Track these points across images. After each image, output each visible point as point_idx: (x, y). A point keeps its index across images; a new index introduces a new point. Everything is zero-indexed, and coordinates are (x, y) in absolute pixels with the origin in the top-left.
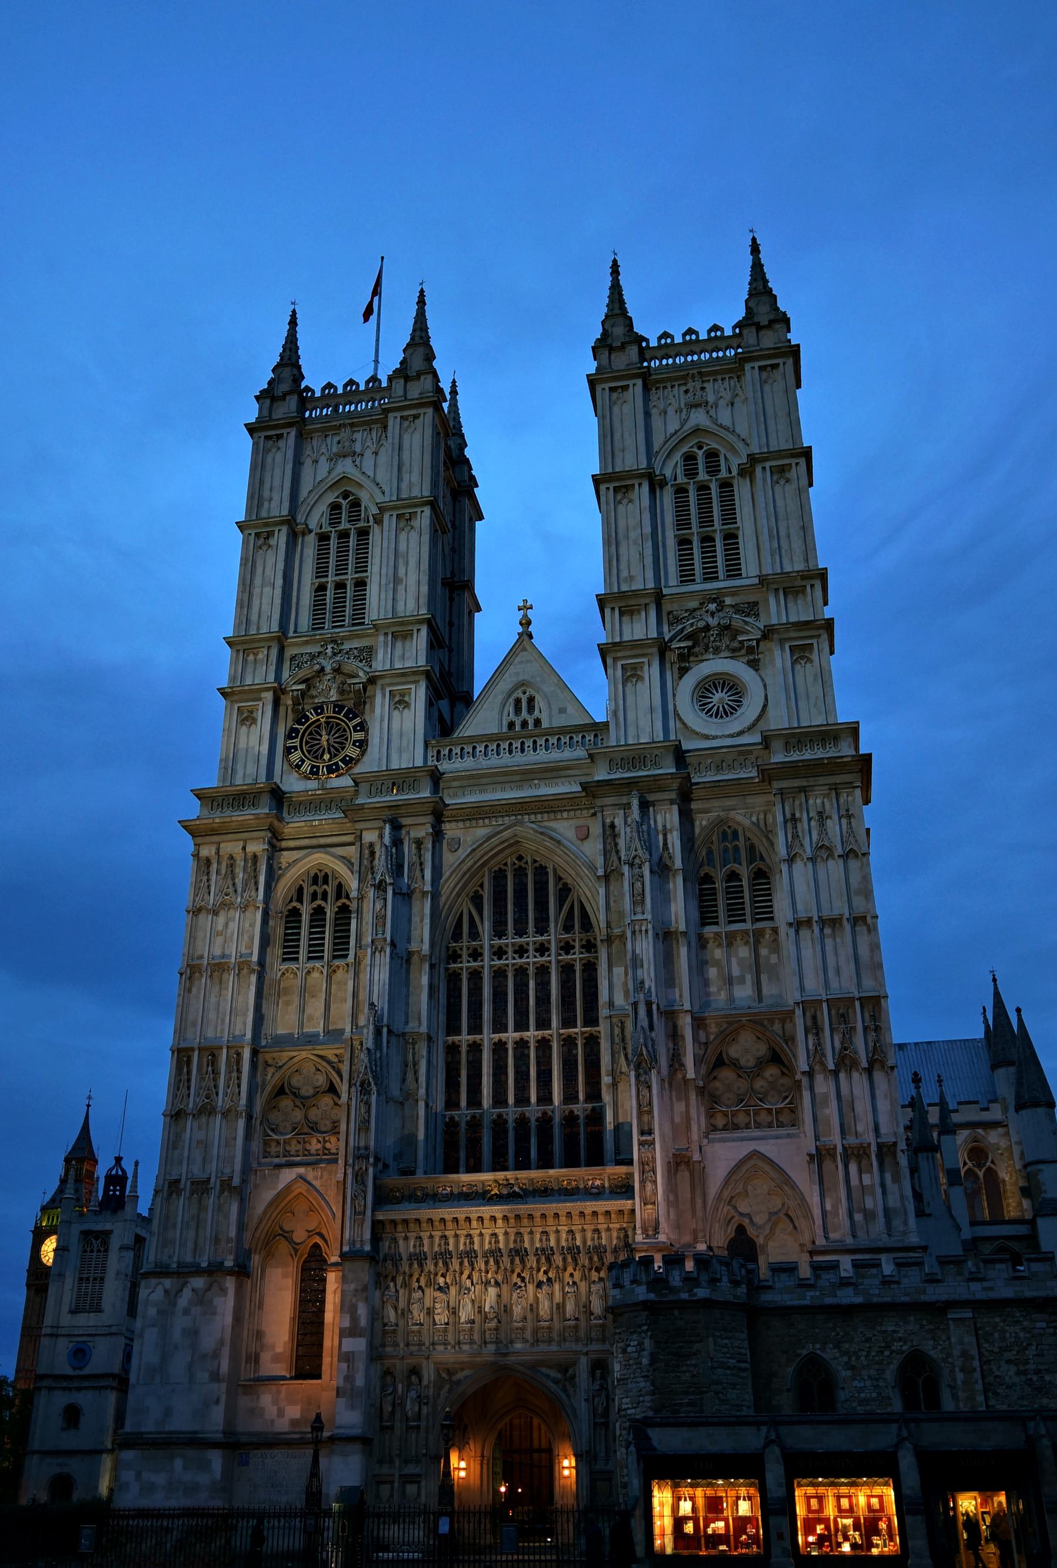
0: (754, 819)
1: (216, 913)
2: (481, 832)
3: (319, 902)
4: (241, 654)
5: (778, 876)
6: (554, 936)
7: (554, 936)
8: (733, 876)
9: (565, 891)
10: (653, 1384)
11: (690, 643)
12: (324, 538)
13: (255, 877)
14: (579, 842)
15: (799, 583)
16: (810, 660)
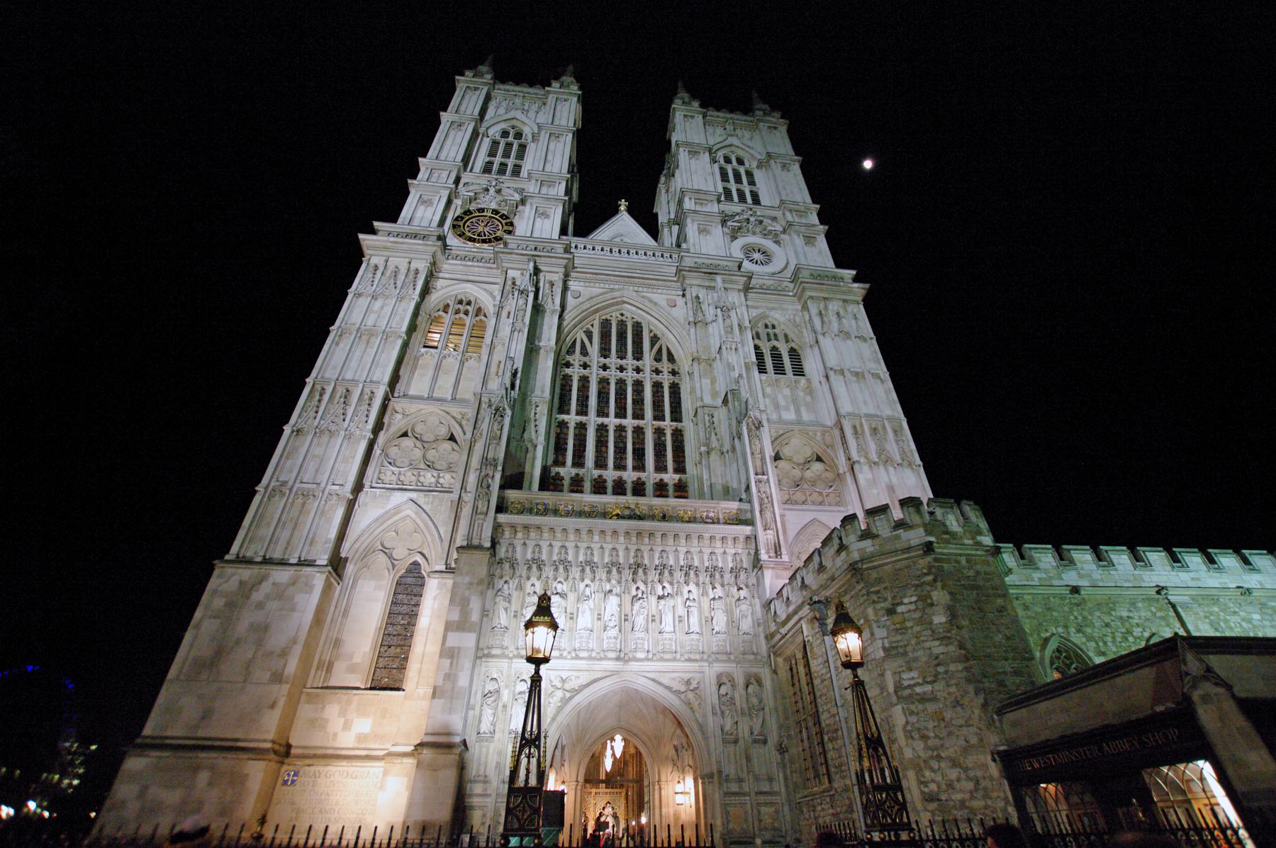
0: (787, 317)
1: (374, 298)
2: (597, 291)
3: (462, 315)
4: (429, 170)
5: (808, 350)
6: (648, 360)
7: (648, 360)
8: (774, 348)
9: (654, 339)
10: (961, 646)
11: (739, 224)
12: (495, 144)
13: (415, 282)
14: (669, 309)
15: (803, 209)
16: (815, 246)
